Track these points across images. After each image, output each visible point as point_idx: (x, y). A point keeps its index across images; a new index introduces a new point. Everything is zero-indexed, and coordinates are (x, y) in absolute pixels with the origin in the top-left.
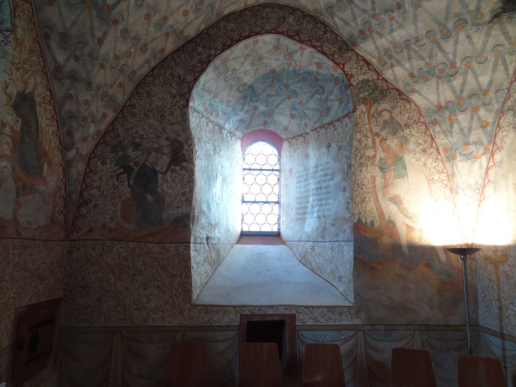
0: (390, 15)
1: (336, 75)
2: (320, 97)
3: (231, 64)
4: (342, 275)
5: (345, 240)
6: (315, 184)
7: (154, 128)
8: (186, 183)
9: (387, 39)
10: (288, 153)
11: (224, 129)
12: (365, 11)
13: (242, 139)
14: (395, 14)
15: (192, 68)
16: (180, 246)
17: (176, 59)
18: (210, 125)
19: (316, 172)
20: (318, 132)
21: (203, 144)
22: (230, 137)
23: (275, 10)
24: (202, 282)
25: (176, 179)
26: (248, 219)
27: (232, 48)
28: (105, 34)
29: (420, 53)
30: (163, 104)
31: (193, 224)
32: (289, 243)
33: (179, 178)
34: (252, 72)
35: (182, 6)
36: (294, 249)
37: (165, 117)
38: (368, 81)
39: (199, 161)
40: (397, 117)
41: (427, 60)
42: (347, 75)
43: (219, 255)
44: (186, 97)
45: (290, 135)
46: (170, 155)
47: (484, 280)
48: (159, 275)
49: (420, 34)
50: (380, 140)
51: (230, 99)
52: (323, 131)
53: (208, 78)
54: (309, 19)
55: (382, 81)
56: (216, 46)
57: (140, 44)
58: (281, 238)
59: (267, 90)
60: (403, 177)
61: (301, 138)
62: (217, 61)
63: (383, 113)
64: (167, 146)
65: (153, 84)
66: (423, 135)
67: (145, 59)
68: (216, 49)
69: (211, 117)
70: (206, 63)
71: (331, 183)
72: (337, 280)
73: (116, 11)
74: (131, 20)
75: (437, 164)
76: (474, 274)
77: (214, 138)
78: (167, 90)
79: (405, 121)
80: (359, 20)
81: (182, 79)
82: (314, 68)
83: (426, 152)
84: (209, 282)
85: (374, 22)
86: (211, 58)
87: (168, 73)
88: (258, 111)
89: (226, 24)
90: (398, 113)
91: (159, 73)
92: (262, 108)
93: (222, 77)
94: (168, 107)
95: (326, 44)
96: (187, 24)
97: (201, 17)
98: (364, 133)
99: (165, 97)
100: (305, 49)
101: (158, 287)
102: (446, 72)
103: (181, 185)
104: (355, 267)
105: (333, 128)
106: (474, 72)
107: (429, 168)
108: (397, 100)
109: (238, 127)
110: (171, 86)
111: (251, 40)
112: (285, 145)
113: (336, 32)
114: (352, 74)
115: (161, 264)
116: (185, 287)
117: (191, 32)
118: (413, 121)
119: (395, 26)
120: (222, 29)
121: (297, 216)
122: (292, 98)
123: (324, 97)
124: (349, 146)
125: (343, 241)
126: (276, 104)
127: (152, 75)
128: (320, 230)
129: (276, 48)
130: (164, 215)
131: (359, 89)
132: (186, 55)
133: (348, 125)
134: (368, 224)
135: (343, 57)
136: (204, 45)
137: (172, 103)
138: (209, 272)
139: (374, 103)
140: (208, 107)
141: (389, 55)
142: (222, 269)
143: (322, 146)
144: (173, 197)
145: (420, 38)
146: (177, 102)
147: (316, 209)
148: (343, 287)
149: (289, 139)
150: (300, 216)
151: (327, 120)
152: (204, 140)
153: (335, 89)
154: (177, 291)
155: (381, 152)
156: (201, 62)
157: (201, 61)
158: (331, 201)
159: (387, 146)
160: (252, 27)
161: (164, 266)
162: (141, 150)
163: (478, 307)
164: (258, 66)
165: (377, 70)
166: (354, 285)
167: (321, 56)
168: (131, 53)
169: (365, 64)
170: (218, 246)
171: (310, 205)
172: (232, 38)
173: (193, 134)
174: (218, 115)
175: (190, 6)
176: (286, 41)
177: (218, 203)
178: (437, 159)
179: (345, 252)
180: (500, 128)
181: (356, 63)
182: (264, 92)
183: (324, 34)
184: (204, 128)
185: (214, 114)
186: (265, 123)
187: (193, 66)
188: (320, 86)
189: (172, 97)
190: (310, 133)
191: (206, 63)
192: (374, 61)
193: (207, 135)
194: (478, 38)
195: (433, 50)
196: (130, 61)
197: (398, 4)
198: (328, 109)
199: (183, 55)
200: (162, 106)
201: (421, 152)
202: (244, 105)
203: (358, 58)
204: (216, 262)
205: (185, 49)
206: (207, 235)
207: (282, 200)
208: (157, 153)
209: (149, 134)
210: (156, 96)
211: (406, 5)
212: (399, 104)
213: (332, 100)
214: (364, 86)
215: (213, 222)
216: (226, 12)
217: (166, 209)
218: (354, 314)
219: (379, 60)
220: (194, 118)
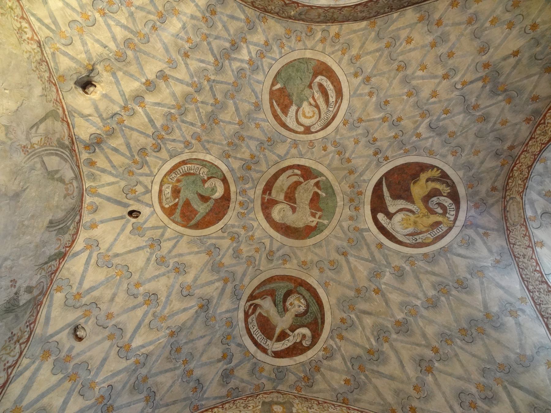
0: (192, 43)
9: (185, 14)
12: (217, 38)
14: (187, 46)
28: (505, 59)
29: (144, 14)
35: (410, 50)
41: (133, 9)
49: (155, 36)
57: (475, 26)
73: (479, 75)
74: (470, 59)
80: (220, 25)
85: (205, 30)
96: (412, 26)
97: (394, 28)
102: (105, 4)
106: (73, 9)
119: (182, 34)
168: (492, 22)
194: (96, 49)
195: (134, 24)
196: (498, 12)
197: (188, 56)
211: (180, 58)
216: (364, 23)
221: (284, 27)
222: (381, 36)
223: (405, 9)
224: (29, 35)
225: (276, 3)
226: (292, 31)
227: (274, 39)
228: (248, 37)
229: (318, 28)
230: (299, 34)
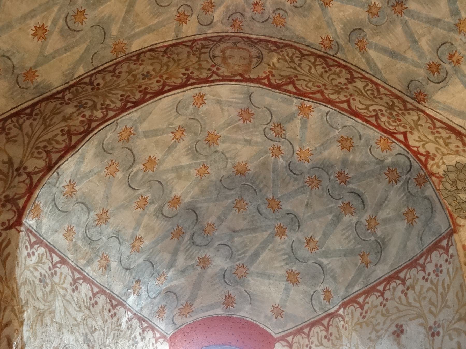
1: (389, 160)
2: (355, 219)
3: (145, 147)
12: (436, 22)
17: (10, 129)
18: (84, 288)
20: (362, 307)
22: (139, 330)
23: (239, 45)
27: (145, 107)
35: (32, 14)
42: (416, 154)
44: (17, 205)
45: (290, 326)
51: (140, 233)
52: (374, 299)
53: (84, 168)
54: (313, 60)
59: (229, 217)
61: (317, 329)
62: (109, 134)
68: (108, 109)
77: (91, 322)
80: (424, 44)
81: (16, 166)
82: (335, 152)
86: (94, 125)
88: (210, 271)
89: (133, 66)
92: (219, 263)
93: (119, 175)
95: (357, 99)
96: (45, 59)
97: (76, 49)
100: (310, 108)
105: (401, 288)
109: (163, 308)
111: (189, 93)
113: (374, 79)
114: (428, 152)
117: (53, 77)
120: (124, 75)
123: (366, 217)
124: (460, 319)
126: (250, 252)
129: (245, 115)
131: (454, 183)
132: (35, 123)
133: (444, 268)
135: (400, 120)
136: (80, 103)
140: (80, 243)
143: (379, 337)
149: (288, 335)
151: (382, 270)
152: (58, 318)
153: (391, 194)
156: (69, 134)
157: (69, 131)
160: (191, 70)
164: (207, 157)
167: (349, 121)
169: (453, 136)
172: (146, 89)
173: (23, 293)
174: (107, 267)
175: (51, 18)
176: (266, 98)
181: (433, 133)
182: (222, 221)
183: (350, 83)
184: (61, 291)
185: (96, 263)
186: (229, 301)
187: (49, 141)
188: (353, 192)
190: (341, 312)
191: (81, 133)
193: (71, 310)
198: (381, 245)
199: (28, 122)
202: (175, 253)
203: (434, 124)
213: (386, 221)
216: (136, 46)
220: (34, 259)
221: (287, 29)
222: (98, 30)
223: (67, 85)
225: (310, 85)
226: (270, 21)
227: (310, 7)
228: (364, 15)
229: (219, 24)
230: (257, 16)
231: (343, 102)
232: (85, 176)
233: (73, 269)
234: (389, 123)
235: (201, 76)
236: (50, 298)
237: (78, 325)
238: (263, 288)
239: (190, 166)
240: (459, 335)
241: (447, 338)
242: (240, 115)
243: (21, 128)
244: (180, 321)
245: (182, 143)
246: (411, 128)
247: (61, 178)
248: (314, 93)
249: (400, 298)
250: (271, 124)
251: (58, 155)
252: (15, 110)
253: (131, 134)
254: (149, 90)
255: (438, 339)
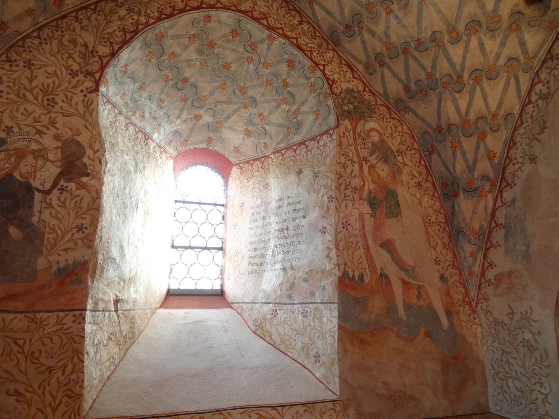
0: (388, 7)
3: (171, 45)
4: (321, 353)
5: (325, 301)
6: (279, 223)
7: (34, 118)
8: (84, 210)
10: (238, 182)
11: (151, 139)
13: (175, 159)
15: (106, 36)
16: (66, 315)
17: (82, 19)
18: (131, 128)
19: (280, 207)
20: (283, 155)
21: (119, 153)
22: (159, 153)
24: (102, 376)
25: (67, 203)
26: (180, 271)
27: (173, 20)
30: (54, 82)
31: (93, 278)
32: (237, 305)
33: (73, 202)
34: (198, 63)
36: (246, 314)
37: (56, 103)
38: (352, 91)
39: (110, 178)
40: (387, 139)
42: (328, 79)
43: (133, 328)
44: (94, 77)
45: (242, 158)
46: (59, 163)
47: (494, 352)
48: (21, 371)
49: (424, 35)
50: (369, 167)
51: (163, 97)
52: (290, 153)
53: (134, 56)
55: (369, 94)
56: (149, 11)
58: (225, 299)
59: (216, 93)
60: (397, 216)
61: (257, 163)
62: (150, 35)
63: (371, 133)
64: (56, 148)
65: (38, 50)
66: (417, 165)
67: (26, 8)
68: (148, 16)
69: (133, 118)
70: (132, 32)
71: (304, 222)
72: (312, 359)
75: (433, 202)
76: (479, 343)
77: (135, 148)
78: (62, 62)
79: (397, 146)
81: (90, 49)
83: (421, 186)
84: (114, 375)
87: (67, 37)
88: (200, 122)
90: (389, 135)
91: (51, 35)
92: (207, 118)
93: (154, 61)
94: (61, 88)
98: (349, 157)
99: (59, 73)
100: (274, 38)
101: (17, 393)
103: (77, 213)
104: (340, 339)
105: (305, 150)
107: (425, 207)
108: (387, 119)
109: (172, 141)
110: (70, 56)
112: (235, 171)
113: (314, 24)
114: (334, 79)
115: (26, 350)
116: (69, 390)
118: (406, 147)
121: (250, 268)
122: (249, 107)
123: (294, 108)
124: (330, 171)
125: (321, 303)
126: (225, 115)
127: (39, 37)
128: (286, 287)
129: (235, 33)
130: (41, 263)
132: (99, 18)
134: (357, 278)
135: (323, 56)
136: (129, 7)
137: (70, 83)
138: (116, 356)
139: (360, 120)
140: (129, 102)
141: (380, 61)
142: (137, 351)
143: (289, 173)
144: (60, 233)
145: (423, 40)
146: (78, 81)
147: (280, 257)
148: (322, 370)
150: (256, 268)
151: (297, 139)
152: (120, 148)
154: (54, 398)
155: (371, 182)
156: (124, 31)
157: (123, 29)
158: (303, 247)
159: (377, 176)
161: (33, 353)
162: (5, 151)
163: (487, 387)
164: (207, 55)
165: (363, 79)
166: (339, 366)
167: (296, 52)
169: (349, 71)
170: (133, 312)
171: (270, 252)
172: (174, 6)
173: (103, 135)
174: (143, 117)
176: (250, 25)
177: (136, 247)
178: (433, 196)
179: (325, 319)
180: (511, 160)
181: (339, 67)
182: (212, 95)
183: (300, 25)
184: (120, 131)
185: (138, 114)
186: (209, 140)
187: (110, 34)
188: (290, 93)
189: (70, 74)
190: (272, 156)
191: (132, 32)
192: (360, 67)
193: (126, 142)
198: (299, 125)
199: (94, 16)
200: (51, 85)
201: (416, 186)
202: (182, 110)
203: (341, 62)
204: (127, 340)
205: (98, 8)
206: (117, 296)
207: (229, 246)
208: (36, 158)
209: (22, 127)
210: (43, 69)
212: (390, 124)
214: (348, 97)
215: (128, 276)
217: (45, 251)
218: (340, 412)
219: (367, 66)
220: (106, 112)
224: (539, 87)
231: (294, 38)
232: (134, 61)
233: (126, 118)
234: (317, 57)
235: (210, 3)
236: (116, 135)
237: (130, 151)
238: (230, 136)
239: (196, 60)
240: (328, 179)
241: (322, 179)
242: (231, 33)
243: (89, 19)
244: (180, 149)
245: (193, 44)
246: (328, 62)
247: (120, 61)
248: (278, 29)
249: (303, 155)
250: (249, 42)
251: (119, 46)
252: (84, 5)
253: (163, 36)
254: (176, 7)
255: (318, 179)
